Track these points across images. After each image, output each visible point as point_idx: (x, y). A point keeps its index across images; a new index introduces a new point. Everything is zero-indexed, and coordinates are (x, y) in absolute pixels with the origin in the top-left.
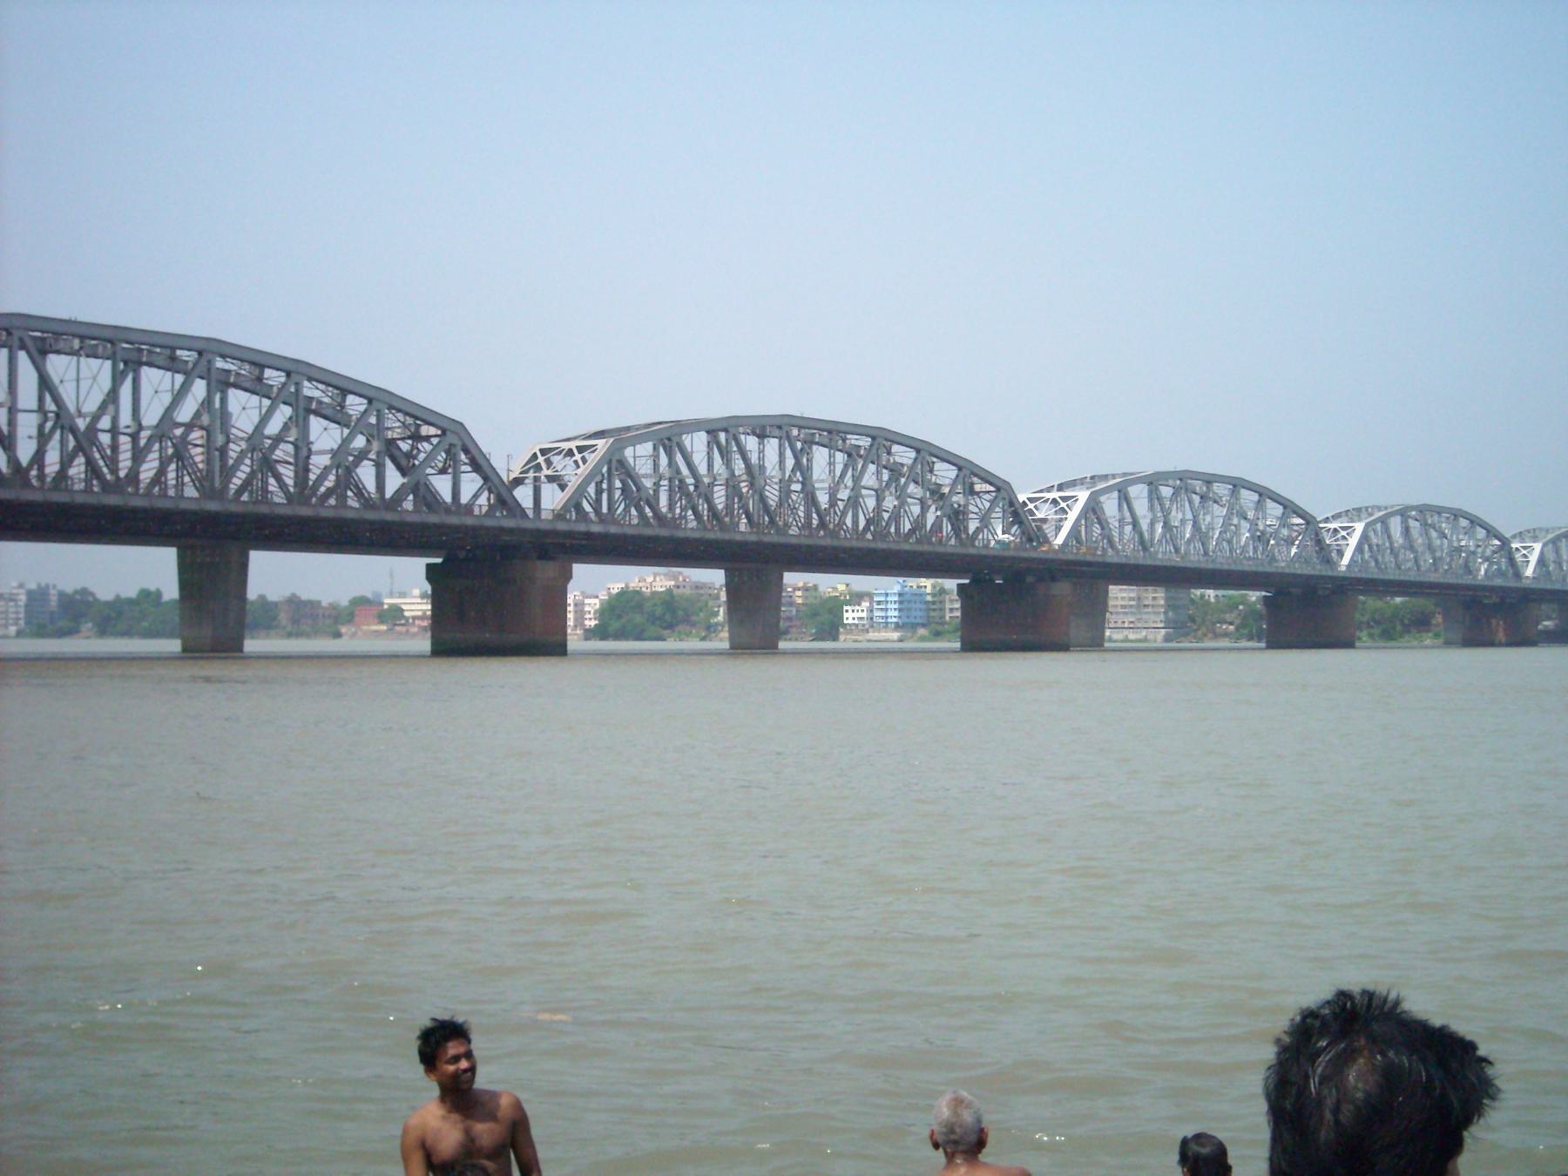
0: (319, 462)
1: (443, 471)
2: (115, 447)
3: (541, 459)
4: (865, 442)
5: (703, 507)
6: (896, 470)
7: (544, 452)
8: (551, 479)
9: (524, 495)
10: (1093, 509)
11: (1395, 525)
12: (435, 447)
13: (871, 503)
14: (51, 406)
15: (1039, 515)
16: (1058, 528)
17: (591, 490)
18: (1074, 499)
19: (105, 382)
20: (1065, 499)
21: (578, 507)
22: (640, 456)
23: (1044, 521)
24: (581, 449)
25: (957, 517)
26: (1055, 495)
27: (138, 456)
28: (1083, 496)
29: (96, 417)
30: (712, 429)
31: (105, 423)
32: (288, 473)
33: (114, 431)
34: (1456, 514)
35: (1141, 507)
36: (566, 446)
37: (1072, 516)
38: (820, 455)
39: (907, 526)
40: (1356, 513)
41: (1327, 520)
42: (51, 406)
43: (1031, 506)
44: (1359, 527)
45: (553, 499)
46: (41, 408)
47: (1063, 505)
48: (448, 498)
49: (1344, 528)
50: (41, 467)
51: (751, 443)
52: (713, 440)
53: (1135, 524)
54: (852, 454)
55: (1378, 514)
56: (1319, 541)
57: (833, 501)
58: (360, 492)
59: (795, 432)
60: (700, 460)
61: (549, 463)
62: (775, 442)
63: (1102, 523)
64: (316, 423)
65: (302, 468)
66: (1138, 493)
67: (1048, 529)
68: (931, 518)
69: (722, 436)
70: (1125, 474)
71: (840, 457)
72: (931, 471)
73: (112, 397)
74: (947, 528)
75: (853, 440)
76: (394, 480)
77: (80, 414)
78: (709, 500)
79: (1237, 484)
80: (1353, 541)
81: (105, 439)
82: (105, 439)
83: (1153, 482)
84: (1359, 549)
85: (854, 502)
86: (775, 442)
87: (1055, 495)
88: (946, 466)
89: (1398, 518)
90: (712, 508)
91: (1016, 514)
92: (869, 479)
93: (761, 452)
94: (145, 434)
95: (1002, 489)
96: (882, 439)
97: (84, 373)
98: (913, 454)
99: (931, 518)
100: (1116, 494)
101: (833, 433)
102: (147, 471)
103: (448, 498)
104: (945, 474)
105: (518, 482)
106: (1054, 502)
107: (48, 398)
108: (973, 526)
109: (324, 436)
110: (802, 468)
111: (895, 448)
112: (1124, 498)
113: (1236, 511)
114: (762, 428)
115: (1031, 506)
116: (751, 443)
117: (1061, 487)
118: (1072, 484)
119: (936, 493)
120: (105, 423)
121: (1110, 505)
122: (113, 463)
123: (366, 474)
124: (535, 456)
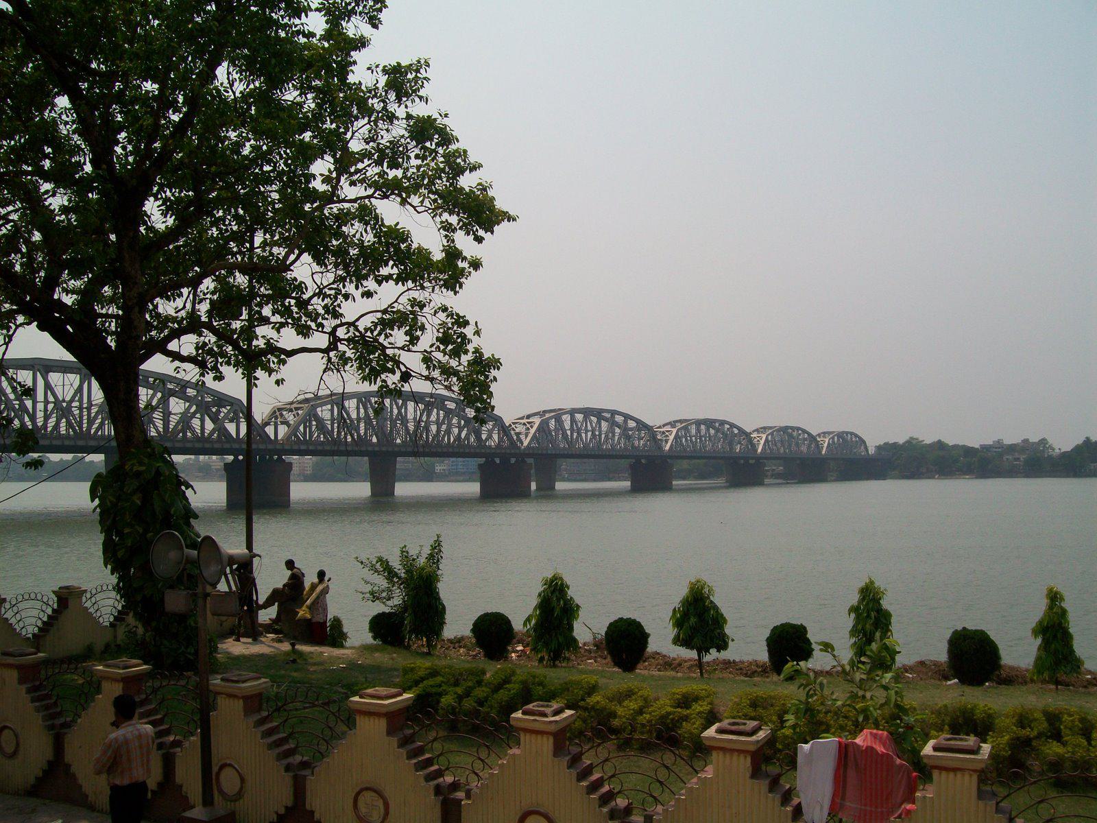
0: (173, 420)
1: (231, 421)
2: (81, 416)
3: (278, 413)
7: (280, 409)
8: (282, 423)
9: (270, 430)
12: (229, 411)
13: (434, 428)
14: (51, 399)
17: (301, 428)
19: (77, 384)
20: (529, 423)
21: (296, 436)
22: (324, 412)
24: (297, 409)
26: (525, 421)
27: (91, 422)
28: (537, 421)
29: (72, 400)
31: (76, 404)
32: (160, 424)
33: (81, 408)
35: (567, 425)
36: (288, 406)
37: (532, 431)
38: (411, 405)
40: (673, 424)
41: (660, 427)
42: (51, 399)
43: (513, 426)
45: (283, 431)
46: (46, 402)
47: (528, 426)
48: (234, 436)
49: (667, 431)
50: (46, 428)
58: (193, 431)
61: (282, 415)
64: (173, 401)
65: (166, 422)
66: (566, 419)
67: (523, 437)
68: (463, 435)
70: (560, 409)
71: (421, 406)
73: (80, 389)
76: (209, 425)
77: (64, 401)
81: (77, 412)
82: (77, 412)
85: (448, 432)
87: (525, 421)
89: (694, 426)
90: (359, 435)
92: (433, 418)
94: (94, 410)
97: (67, 382)
99: (463, 435)
102: (52, 422)
103: (234, 436)
105: (267, 424)
106: (524, 424)
107: (49, 393)
108: (484, 437)
109: (177, 406)
113: (613, 424)
115: (513, 426)
117: (528, 417)
120: (76, 404)
121: (552, 423)
122: (80, 424)
123: (196, 423)
124: (275, 412)
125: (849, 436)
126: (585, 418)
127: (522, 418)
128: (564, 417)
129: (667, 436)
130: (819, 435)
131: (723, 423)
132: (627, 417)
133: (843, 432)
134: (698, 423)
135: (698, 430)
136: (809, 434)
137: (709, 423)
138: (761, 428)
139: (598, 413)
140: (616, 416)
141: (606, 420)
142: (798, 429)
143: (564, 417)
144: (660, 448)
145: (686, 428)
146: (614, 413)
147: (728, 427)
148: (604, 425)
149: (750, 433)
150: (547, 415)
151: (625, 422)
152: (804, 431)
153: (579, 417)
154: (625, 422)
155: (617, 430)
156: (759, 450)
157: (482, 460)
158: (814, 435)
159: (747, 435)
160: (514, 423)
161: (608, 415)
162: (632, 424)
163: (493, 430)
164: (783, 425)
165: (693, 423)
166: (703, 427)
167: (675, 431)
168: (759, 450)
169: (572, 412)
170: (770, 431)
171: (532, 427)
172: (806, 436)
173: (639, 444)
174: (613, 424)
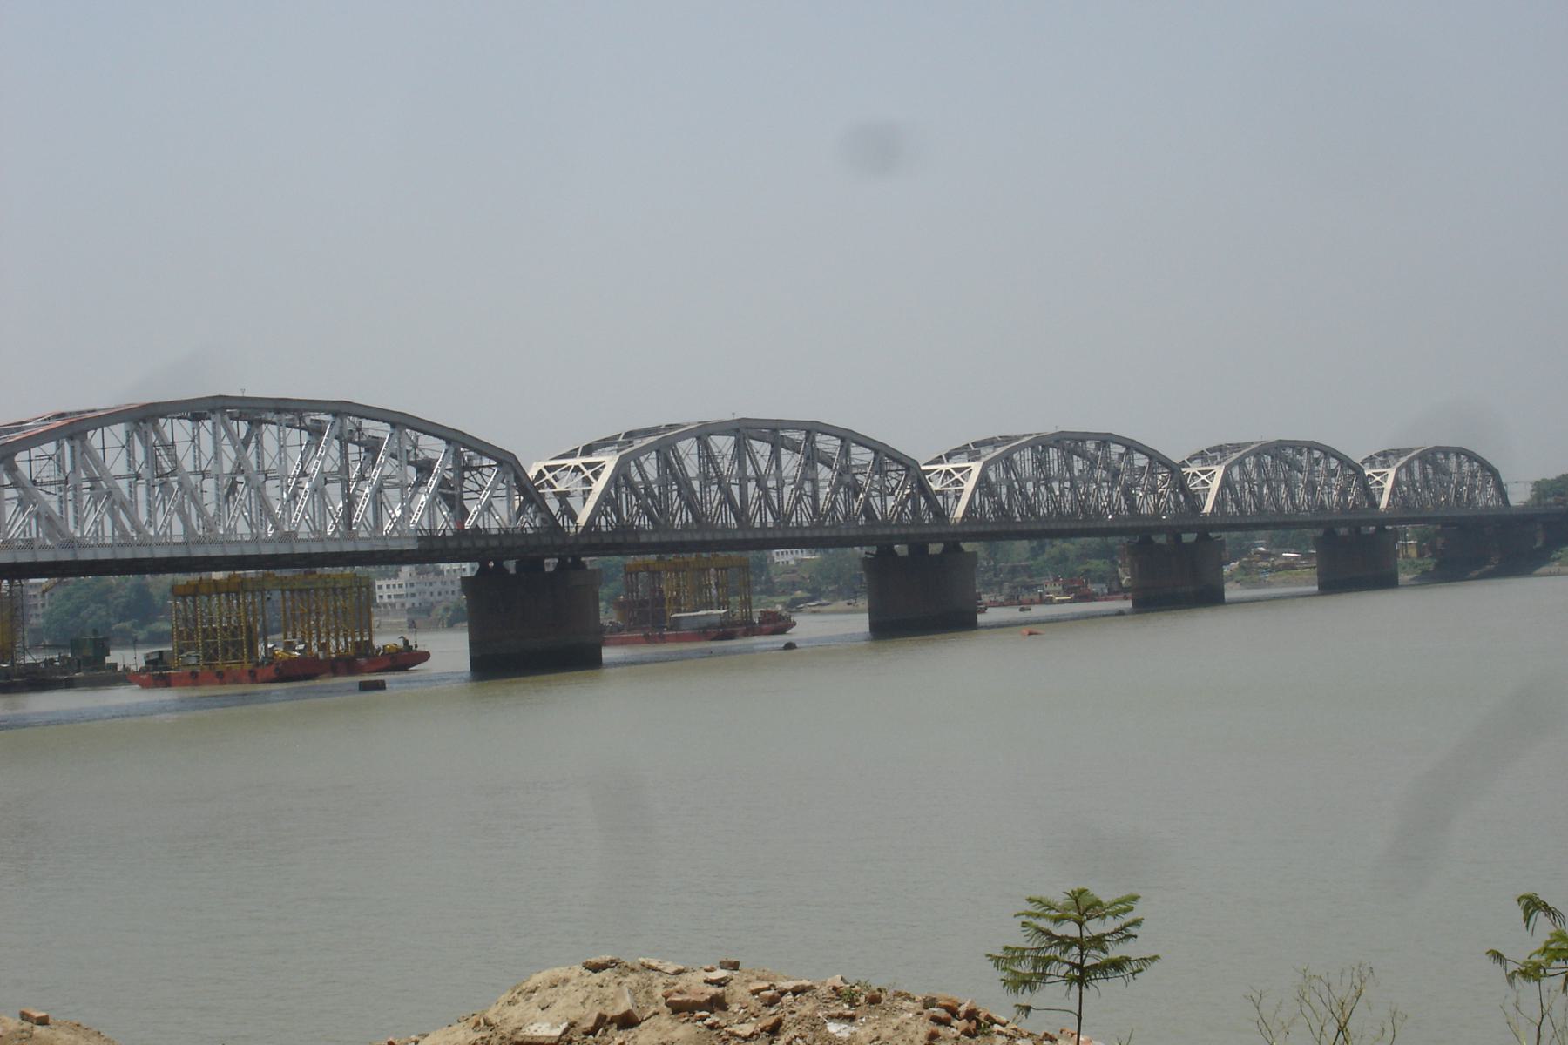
20: (588, 466)
26: (578, 461)
28: (609, 461)
35: (692, 467)
37: (599, 486)
40: (972, 450)
43: (549, 476)
47: (588, 473)
49: (958, 470)
66: (688, 448)
70: (670, 427)
87: (578, 461)
89: (1028, 453)
91: (530, 492)
100: (654, 454)
106: (577, 469)
113: (813, 458)
115: (549, 476)
117: (588, 450)
125: (1453, 459)
126: (741, 450)
129: (958, 482)
130: (1371, 461)
131: (1105, 440)
132: (848, 438)
133: (1436, 450)
134: (1040, 444)
135: (1041, 463)
136: (1344, 461)
137: (1069, 443)
138: (1212, 450)
139: (773, 432)
140: (819, 437)
141: (795, 448)
142: (1311, 446)
144: (941, 514)
145: (1007, 461)
146: (812, 429)
147: (1123, 450)
148: (791, 463)
149: (1183, 464)
150: (638, 444)
151: (845, 451)
152: (1328, 452)
153: (723, 444)
154: (845, 451)
155: (824, 473)
156: (1208, 508)
157: (468, 569)
158: (1358, 461)
159: (1174, 469)
160: (550, 469)
161: (799, 436)
162: (862, 456)
164: (1271, 436)
165: (1020, 448)
166: (1053, 453)
167: (976, 467)
168: (1208, 508)
169: (702, 434)
170: (1235, 456)
171: (596, 475)
172: (1334, 463)
173: (884, 506)
174: (813, 458)
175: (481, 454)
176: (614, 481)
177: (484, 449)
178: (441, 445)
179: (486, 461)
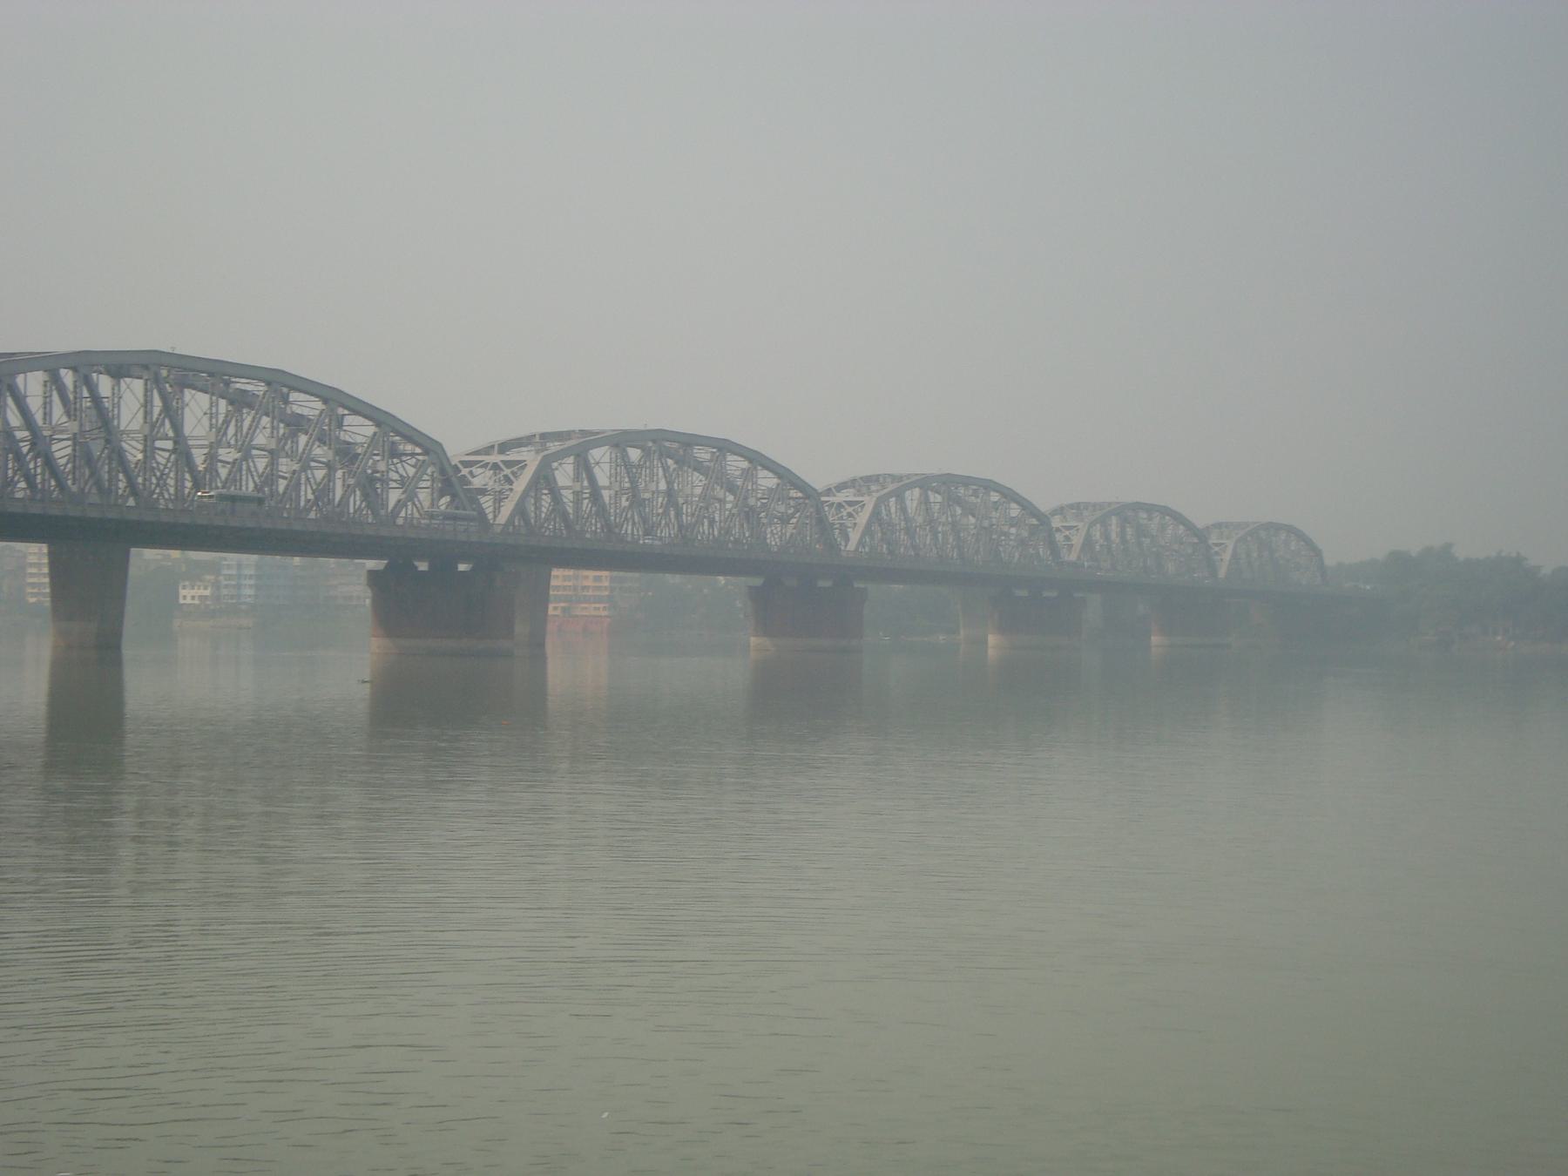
4: (259, 388)
5: (36, 466)
6: (297, 424)
10: (544, 479)
11: (912, 497)
13: (261, 464)
15: (477, 483)
16: (499, 499)
18: (521, 465)
20: (509, 464)
23: (483, 492)
25: (371, 486)
28: (530, 458)
30: (50, 364)
34: (989, 486)
35: (602, 478)
37: (520, 485)
39: (307, 494)
41: (828, 492)
43: (465, 471)
44: (870, 502)
47: (507, 471)
49: (850, 504)
51: (104, 384)
52: (55, 380)
53: (596, 496)
54: (240, 402)
55: (891, 487)
56: (821, 521)
57: (212, 458)
59: (164, 373)
60: (35, 404)
62: (138, 385)
63: (555, 493)
66: (599, 454)
67: (487, 503)
69: (68, 377)
70: (583, 433)
72: (340, 425)
74: (356, 501)
75: (241, 384)
78: (49, 462)
79: (724, 447)
80: (863, 518)
83: (620, 441)
84: (868, 530)
86: (138, 385)
88: (359, 420)
89: (917, 491)
91: (450, 480)
93: (117, 396)
95: (431, 448)
96: (281, 383)
98: (319, 405)
100: (571, 459)
101: (214, 376)
104: (359, 430)
106: (495, 467)
108: (394, 496)
110: (172, 413)
111: (294, 396)
112: (584, 467)
114: (120, 366)
115: (465, 471)
116: (104, 384)
117: (504, 447)
118: (518, 443)
119: (347, 454)
121: (564, 474)
127: (488, 450)
128: (597, 454)
138: (1071, 506)
140: (730, 457)
141: (699, 467)
143: (597, 454)
145: (899, 495)
150: (554, 447)
159: (1043, 519)
160: (467, 464)
163: (418, 477)
175: (408, 439)
176: (534, 484)
177: (412, 435)
178: (369, 429)
179: (409, 448)
